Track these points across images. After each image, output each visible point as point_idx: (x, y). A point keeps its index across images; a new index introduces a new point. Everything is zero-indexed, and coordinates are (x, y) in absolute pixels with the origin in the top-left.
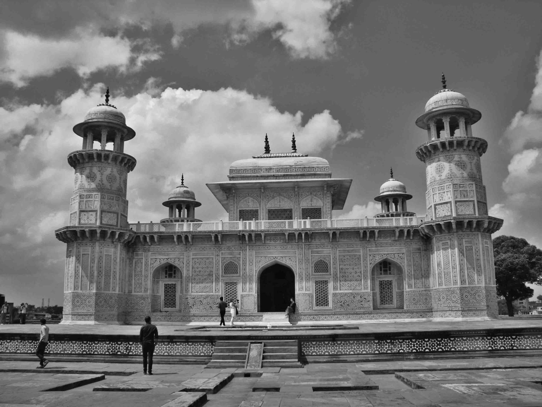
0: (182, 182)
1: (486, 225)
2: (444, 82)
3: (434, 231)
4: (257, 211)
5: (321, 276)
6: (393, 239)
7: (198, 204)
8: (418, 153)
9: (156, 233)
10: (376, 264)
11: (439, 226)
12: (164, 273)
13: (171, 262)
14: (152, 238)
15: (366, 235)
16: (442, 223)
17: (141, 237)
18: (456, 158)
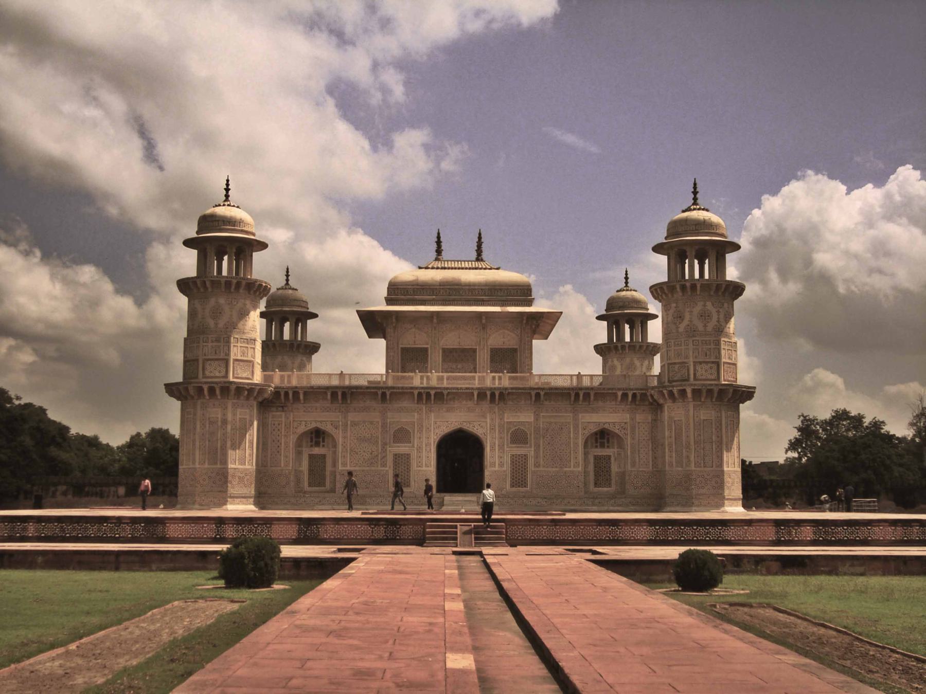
0: (287, 280)
1: (730, 395)
2: (695, 193)
3: (665, 399)
4: (426, 350)
5: (520, 451)
6: (614, 403)
7: (315, 316)
8: (652, 292)
9: (302, 388)
10: (592, 434)
11: (671, 394)
12: (309, 440)
13: (322, 427)
14: (296, 393)
15: (577, 395)
16: (675, 391)
17: (282, 394)
18: (700, 304)
